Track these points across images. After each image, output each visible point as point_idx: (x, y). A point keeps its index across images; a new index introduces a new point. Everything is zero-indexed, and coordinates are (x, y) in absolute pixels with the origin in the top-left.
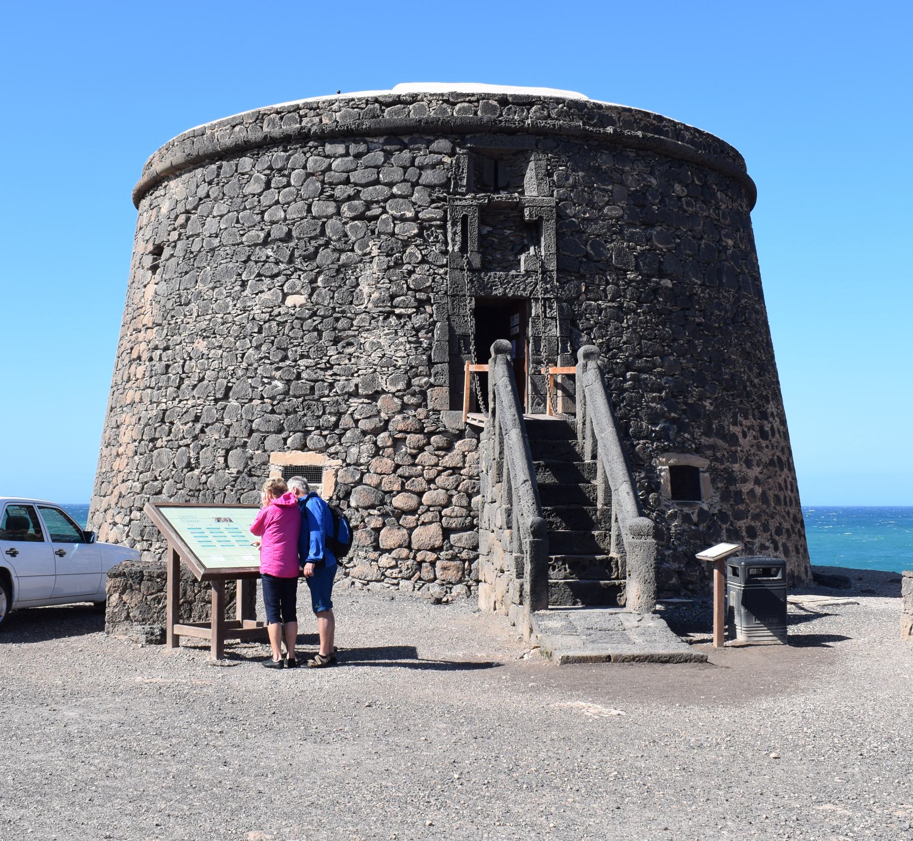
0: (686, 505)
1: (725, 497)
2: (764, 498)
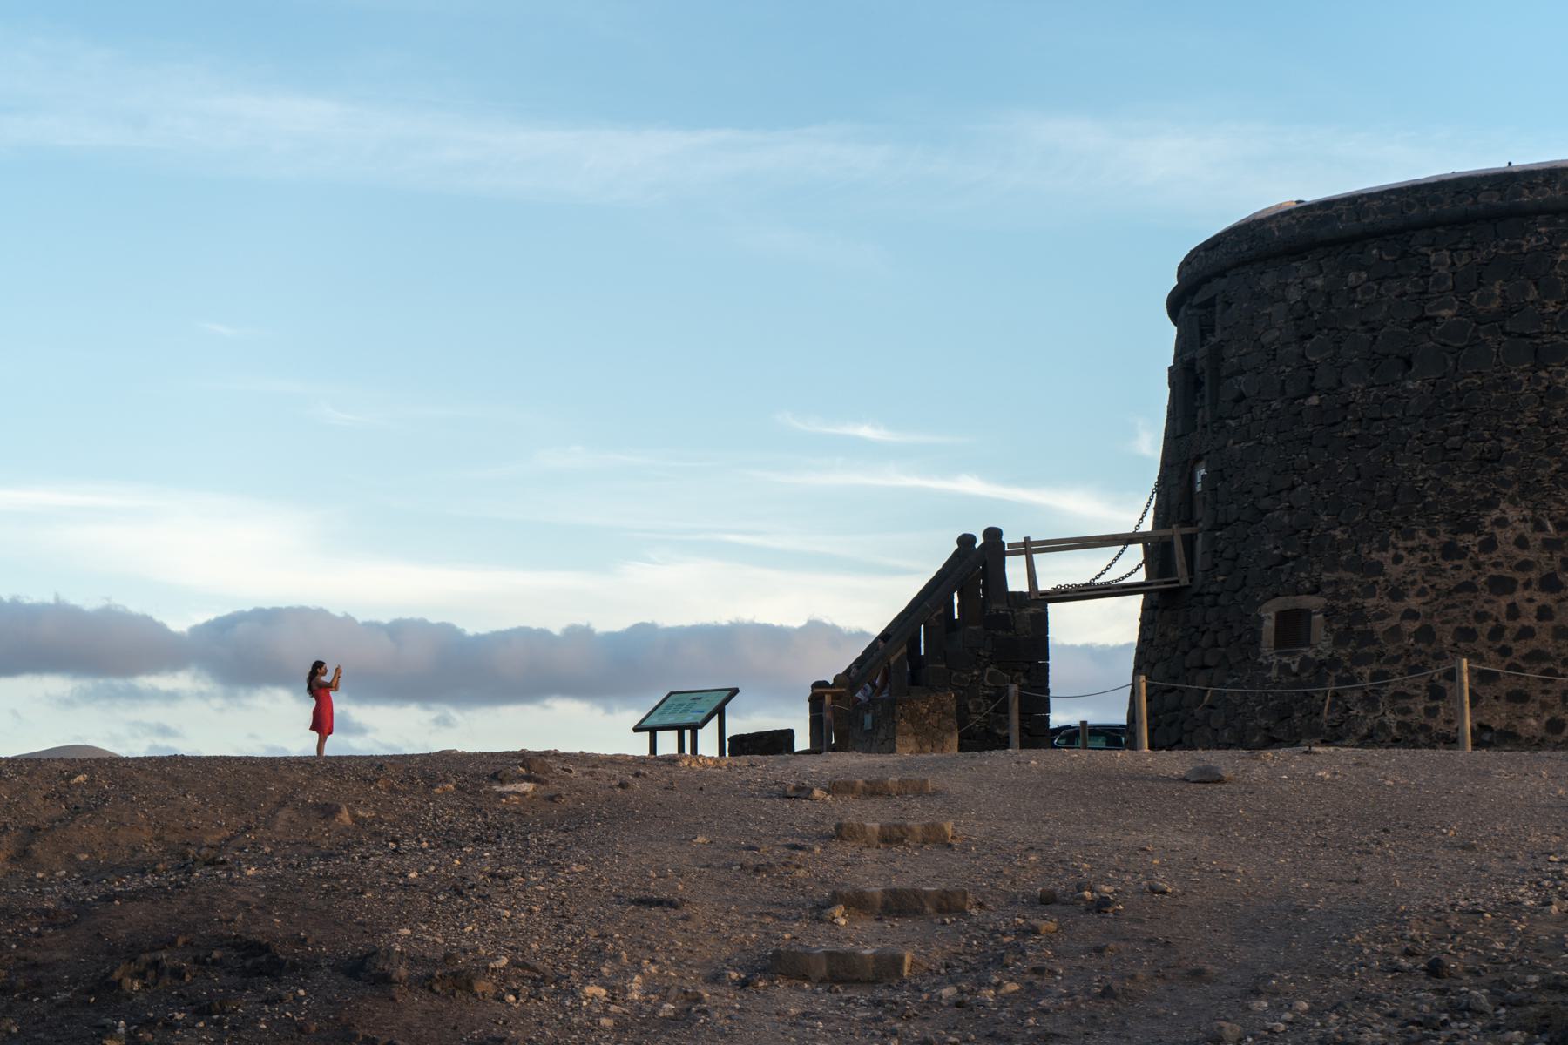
0: (1285, 654)
1: (1340, 640)
2: (1426, 634)
